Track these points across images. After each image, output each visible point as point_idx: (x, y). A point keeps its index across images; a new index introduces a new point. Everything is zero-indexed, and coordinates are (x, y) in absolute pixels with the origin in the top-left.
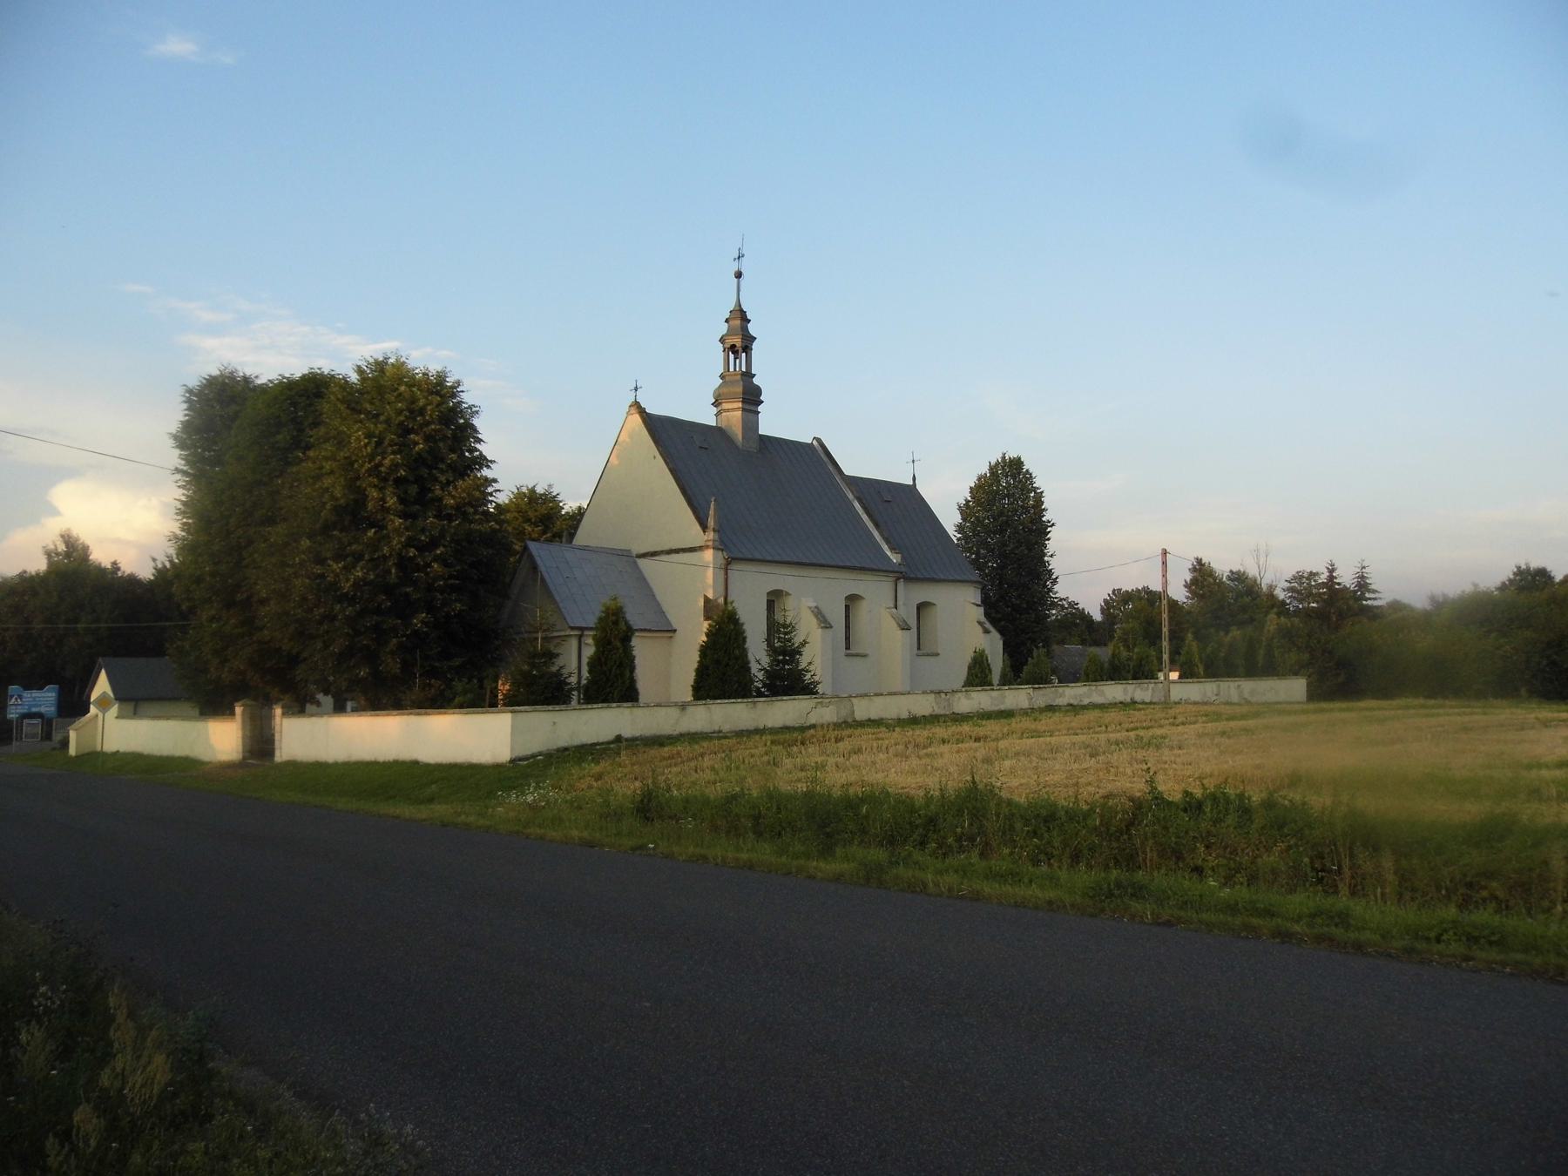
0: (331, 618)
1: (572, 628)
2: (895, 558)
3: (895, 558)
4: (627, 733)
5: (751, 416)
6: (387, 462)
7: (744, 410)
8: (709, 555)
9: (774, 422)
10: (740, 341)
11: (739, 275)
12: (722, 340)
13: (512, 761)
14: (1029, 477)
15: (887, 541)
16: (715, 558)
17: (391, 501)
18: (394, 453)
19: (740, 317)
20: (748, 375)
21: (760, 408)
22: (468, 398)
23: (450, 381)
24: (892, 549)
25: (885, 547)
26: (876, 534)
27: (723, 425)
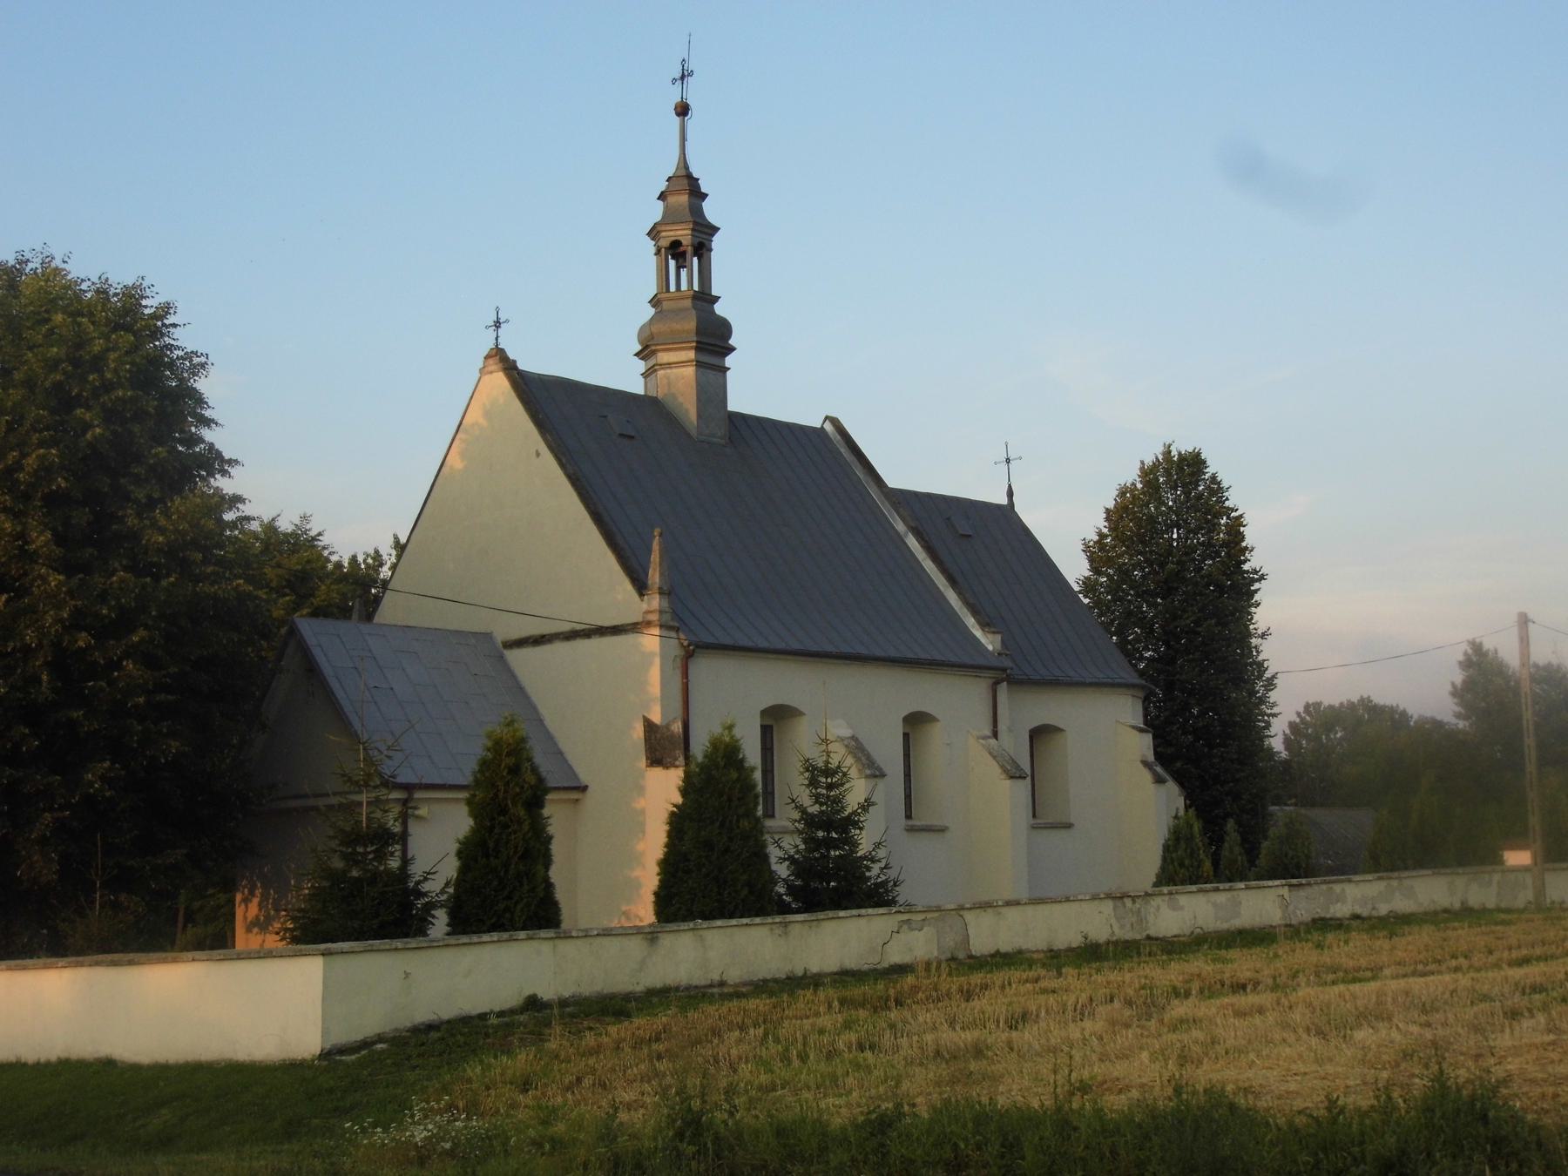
2: (989, 642)
3: (989, 642)
4: (547, 993)
5: (711, 375)
6: (31, 462)
7: (699, 364)
8: (651, 641)
9: (754, 388)
10: (686, 235)
11: (683, 110)
12: (654, 233)
13: (326, 1055)
14: (1216, 487)
15: (975, 612)
16: (662, 647)
17: (40, 539)
18: (41, 444)
19: (686, 189)
20: (704, 298)
21: (729, 361)
22: (185, 337)
23: (150, 304)
24: (985, 625)
25: (970, 622)
26: (952, 597)
27: (652, 393)
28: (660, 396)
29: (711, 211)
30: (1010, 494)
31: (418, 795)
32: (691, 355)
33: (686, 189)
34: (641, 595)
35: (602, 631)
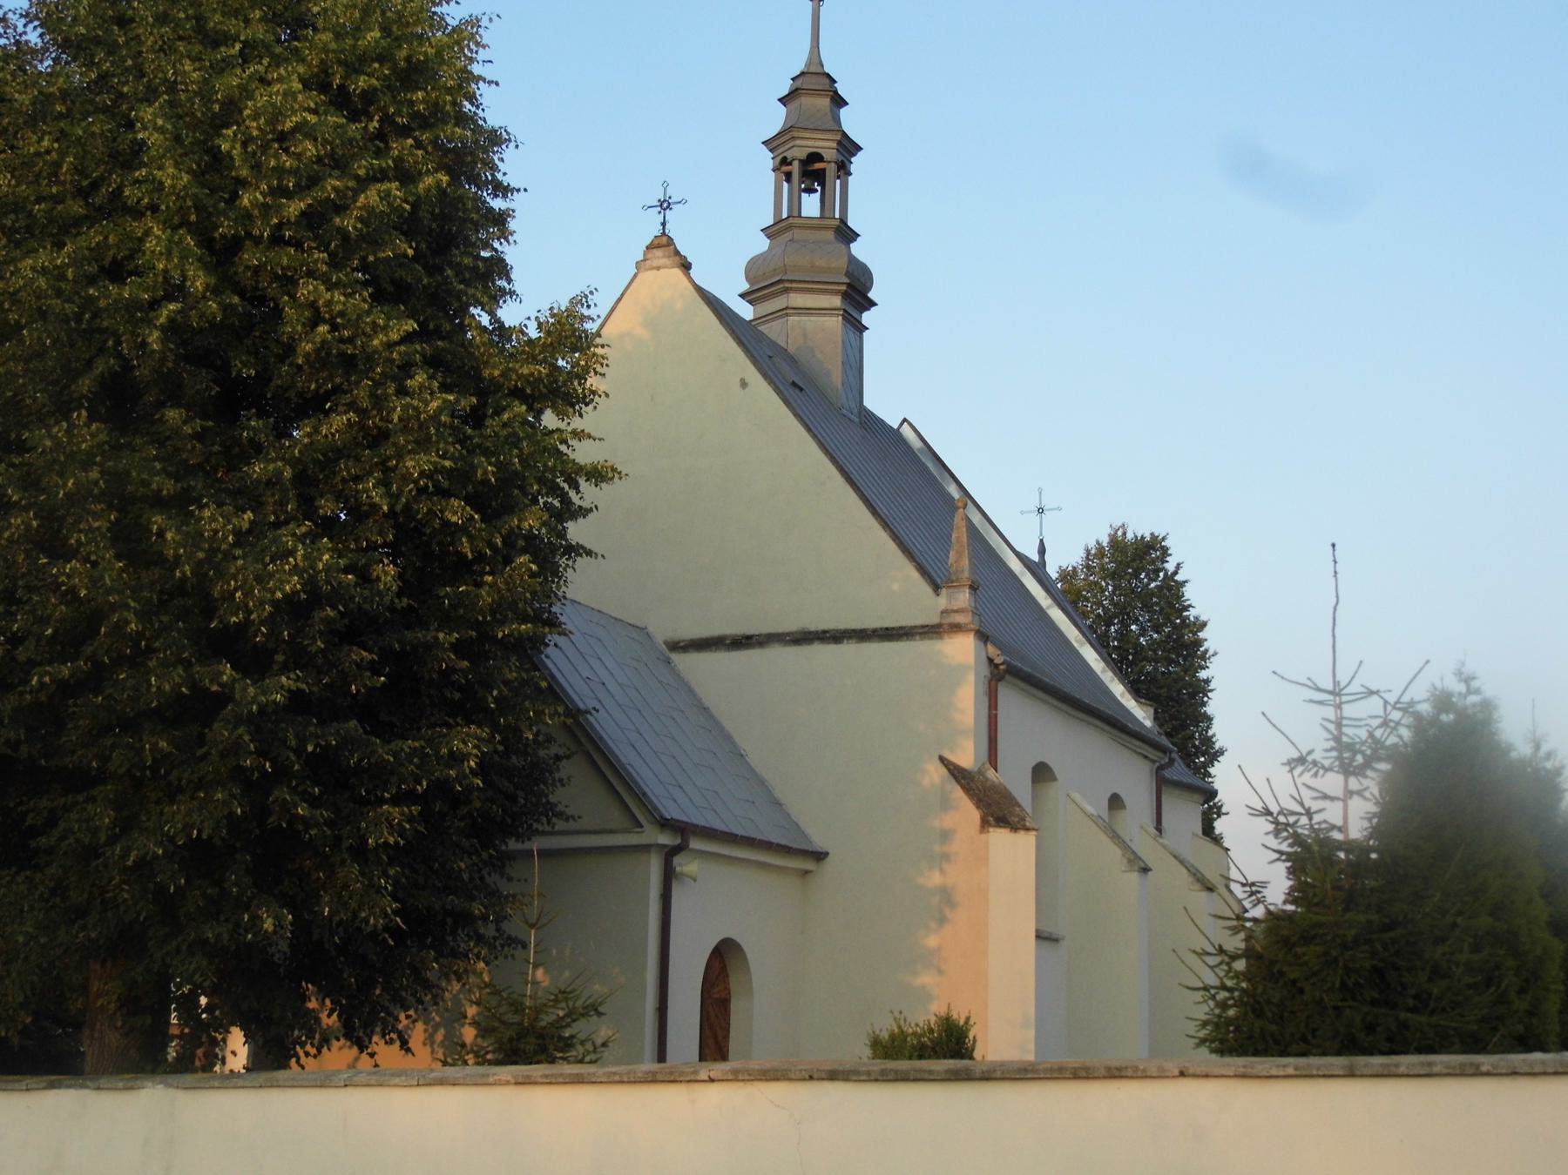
0: (203, 706)
1: (665, 824)
8: (962, 650)
10: (814, 152)
19: (815, 92)
21: (867, 318)
24: (1136, 690)
28: (791, 349)
29: (850, 120)
30: (1042, 550)
31: (695, 844)
32: (837, 301)
33: (815, 92)
34: (937, 588)
35: (862, 635)
